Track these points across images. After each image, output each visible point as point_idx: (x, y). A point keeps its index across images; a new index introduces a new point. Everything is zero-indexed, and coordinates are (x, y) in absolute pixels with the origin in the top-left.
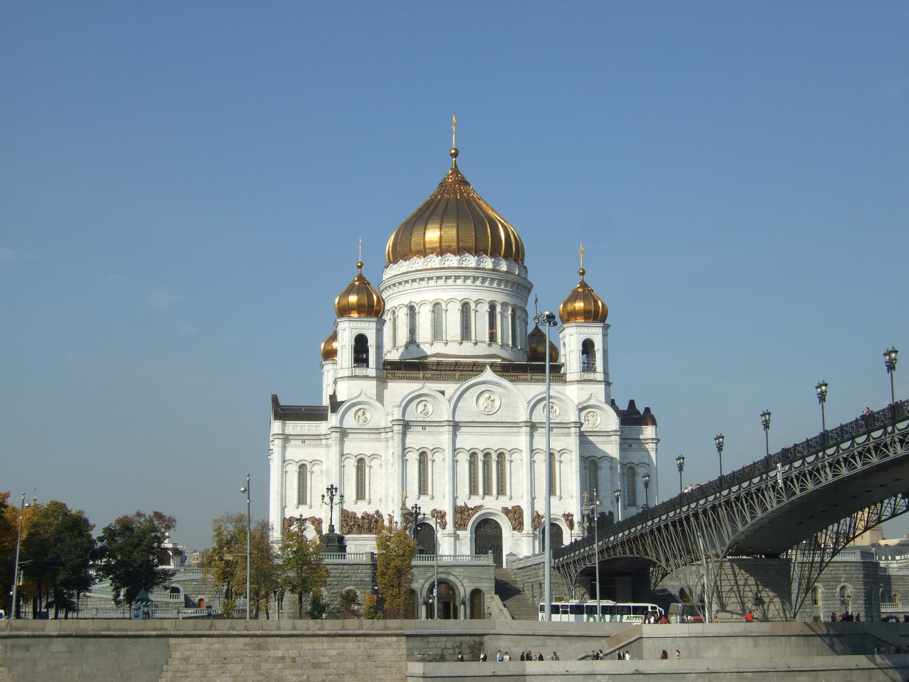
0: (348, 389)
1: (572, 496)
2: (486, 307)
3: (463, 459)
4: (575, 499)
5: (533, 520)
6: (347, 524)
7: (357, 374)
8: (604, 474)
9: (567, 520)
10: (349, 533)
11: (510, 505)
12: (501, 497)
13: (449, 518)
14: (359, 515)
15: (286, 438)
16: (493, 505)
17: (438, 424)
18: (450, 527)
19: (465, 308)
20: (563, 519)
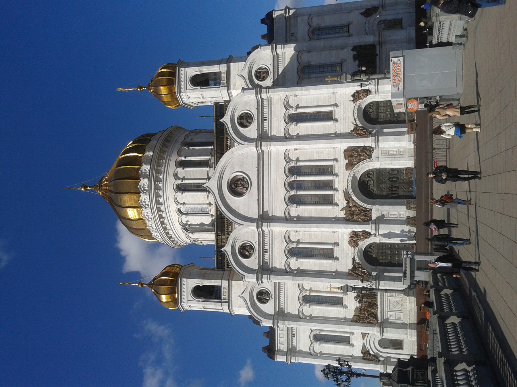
0: (239, 307)
1: (334, 93)
2: (180, 170)
3: (295, 211)
4: (336, 90)
5: (360, 136)
6: (367, 318)
7: (227, 297)
8: (315, 59)
9: (360, 98)
10: (376, 317)
11: (343, 162)
12: (336, 170)
13: (358, 228)
14: (358, 305)
15: (292, 351)
16: (342, 180)
17: (262, 236)
18: (369, 228)
19: (181, 188)
20: (359, 102)
